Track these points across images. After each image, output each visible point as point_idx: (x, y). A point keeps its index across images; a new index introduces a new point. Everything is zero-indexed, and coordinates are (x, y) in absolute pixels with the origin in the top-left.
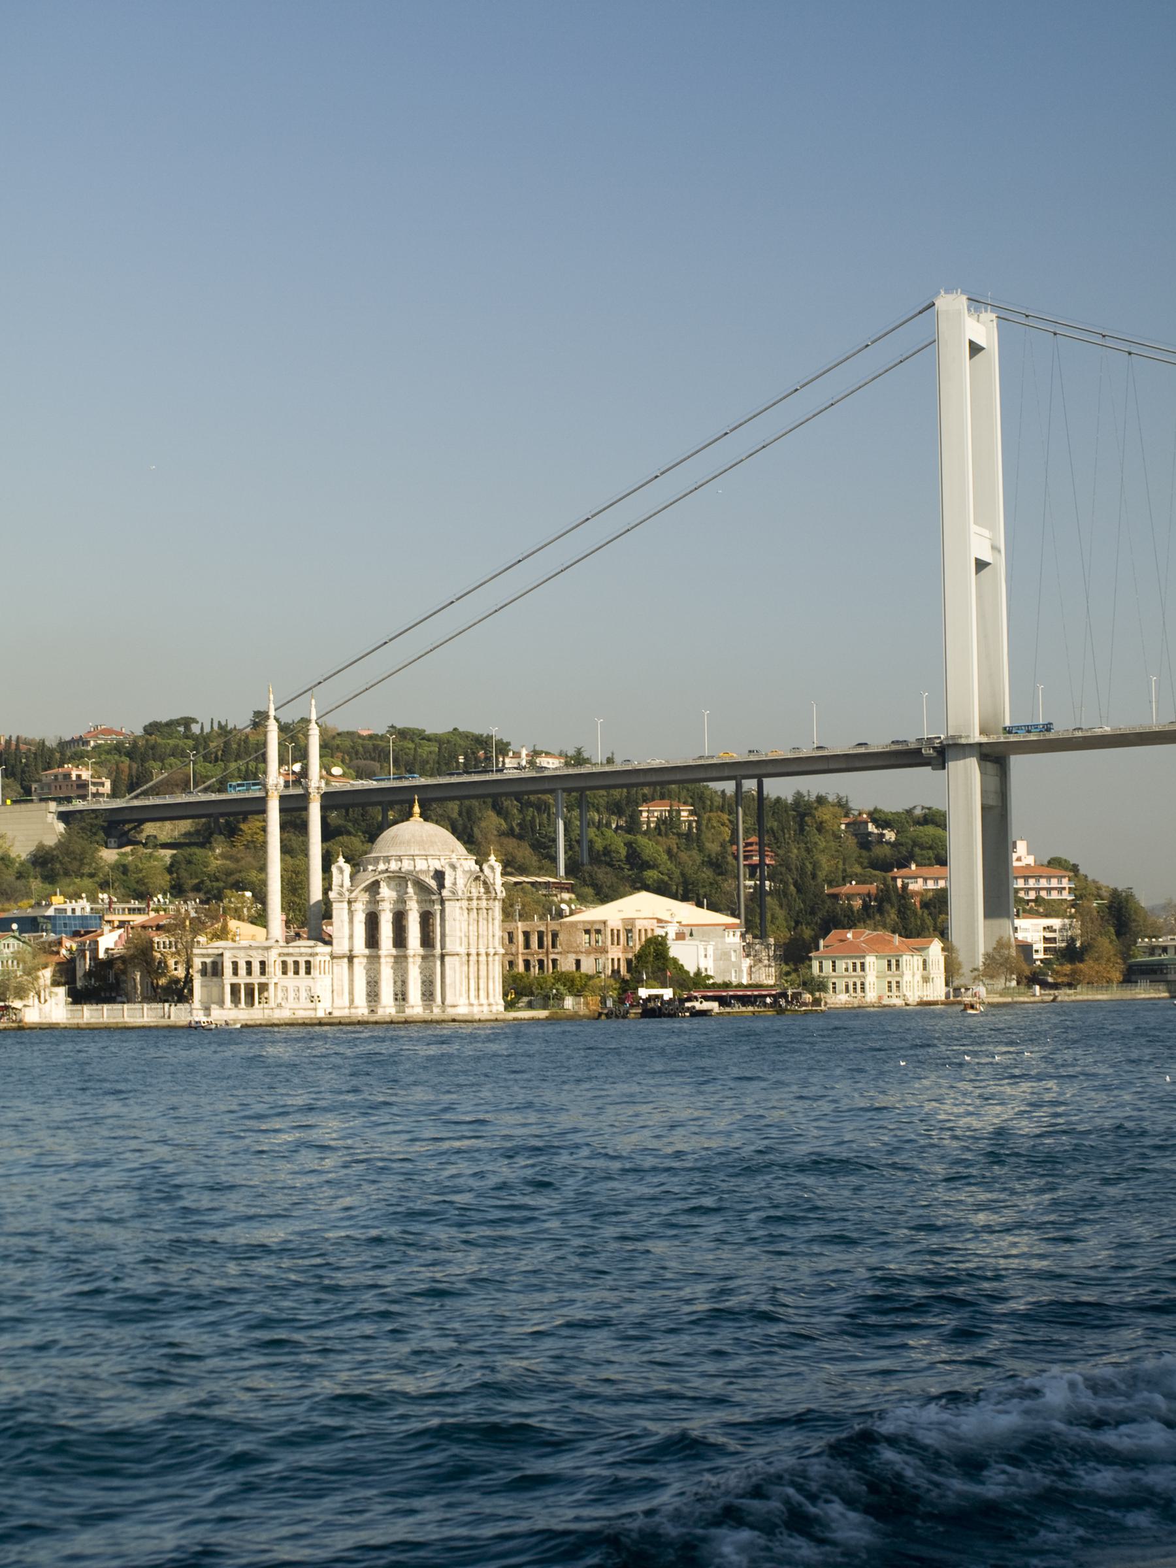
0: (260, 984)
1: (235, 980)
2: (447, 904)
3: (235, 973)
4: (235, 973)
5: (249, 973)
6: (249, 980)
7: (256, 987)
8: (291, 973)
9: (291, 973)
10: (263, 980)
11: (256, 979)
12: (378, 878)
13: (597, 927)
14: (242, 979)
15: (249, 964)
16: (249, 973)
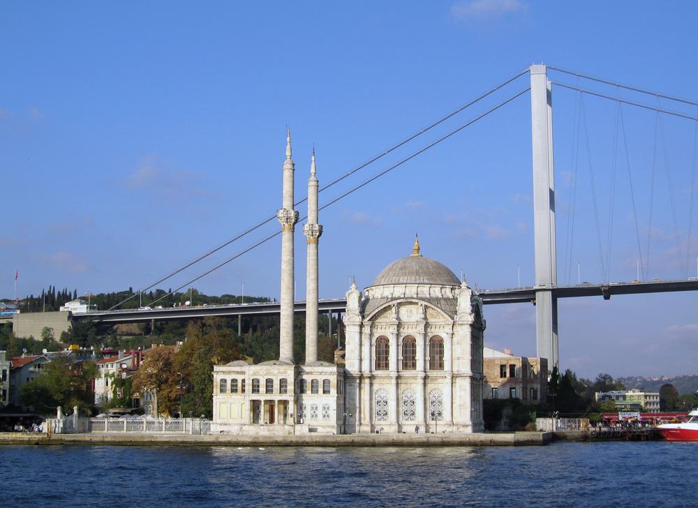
0: (280, 402)
1: (255, 397)
2: (457, 328)
3: (255, 389)
4: (255, 389)
5: (269, 389)
6: (269, 397)
7: (276, 402)
8: (309, 392)
9: (309, 392)
10: (284, 397)
11: (276, 397)
12: (390, 303)
13: (512, 363)
14: (262, 397)
15: (269, 383)
16: (269, 389)
